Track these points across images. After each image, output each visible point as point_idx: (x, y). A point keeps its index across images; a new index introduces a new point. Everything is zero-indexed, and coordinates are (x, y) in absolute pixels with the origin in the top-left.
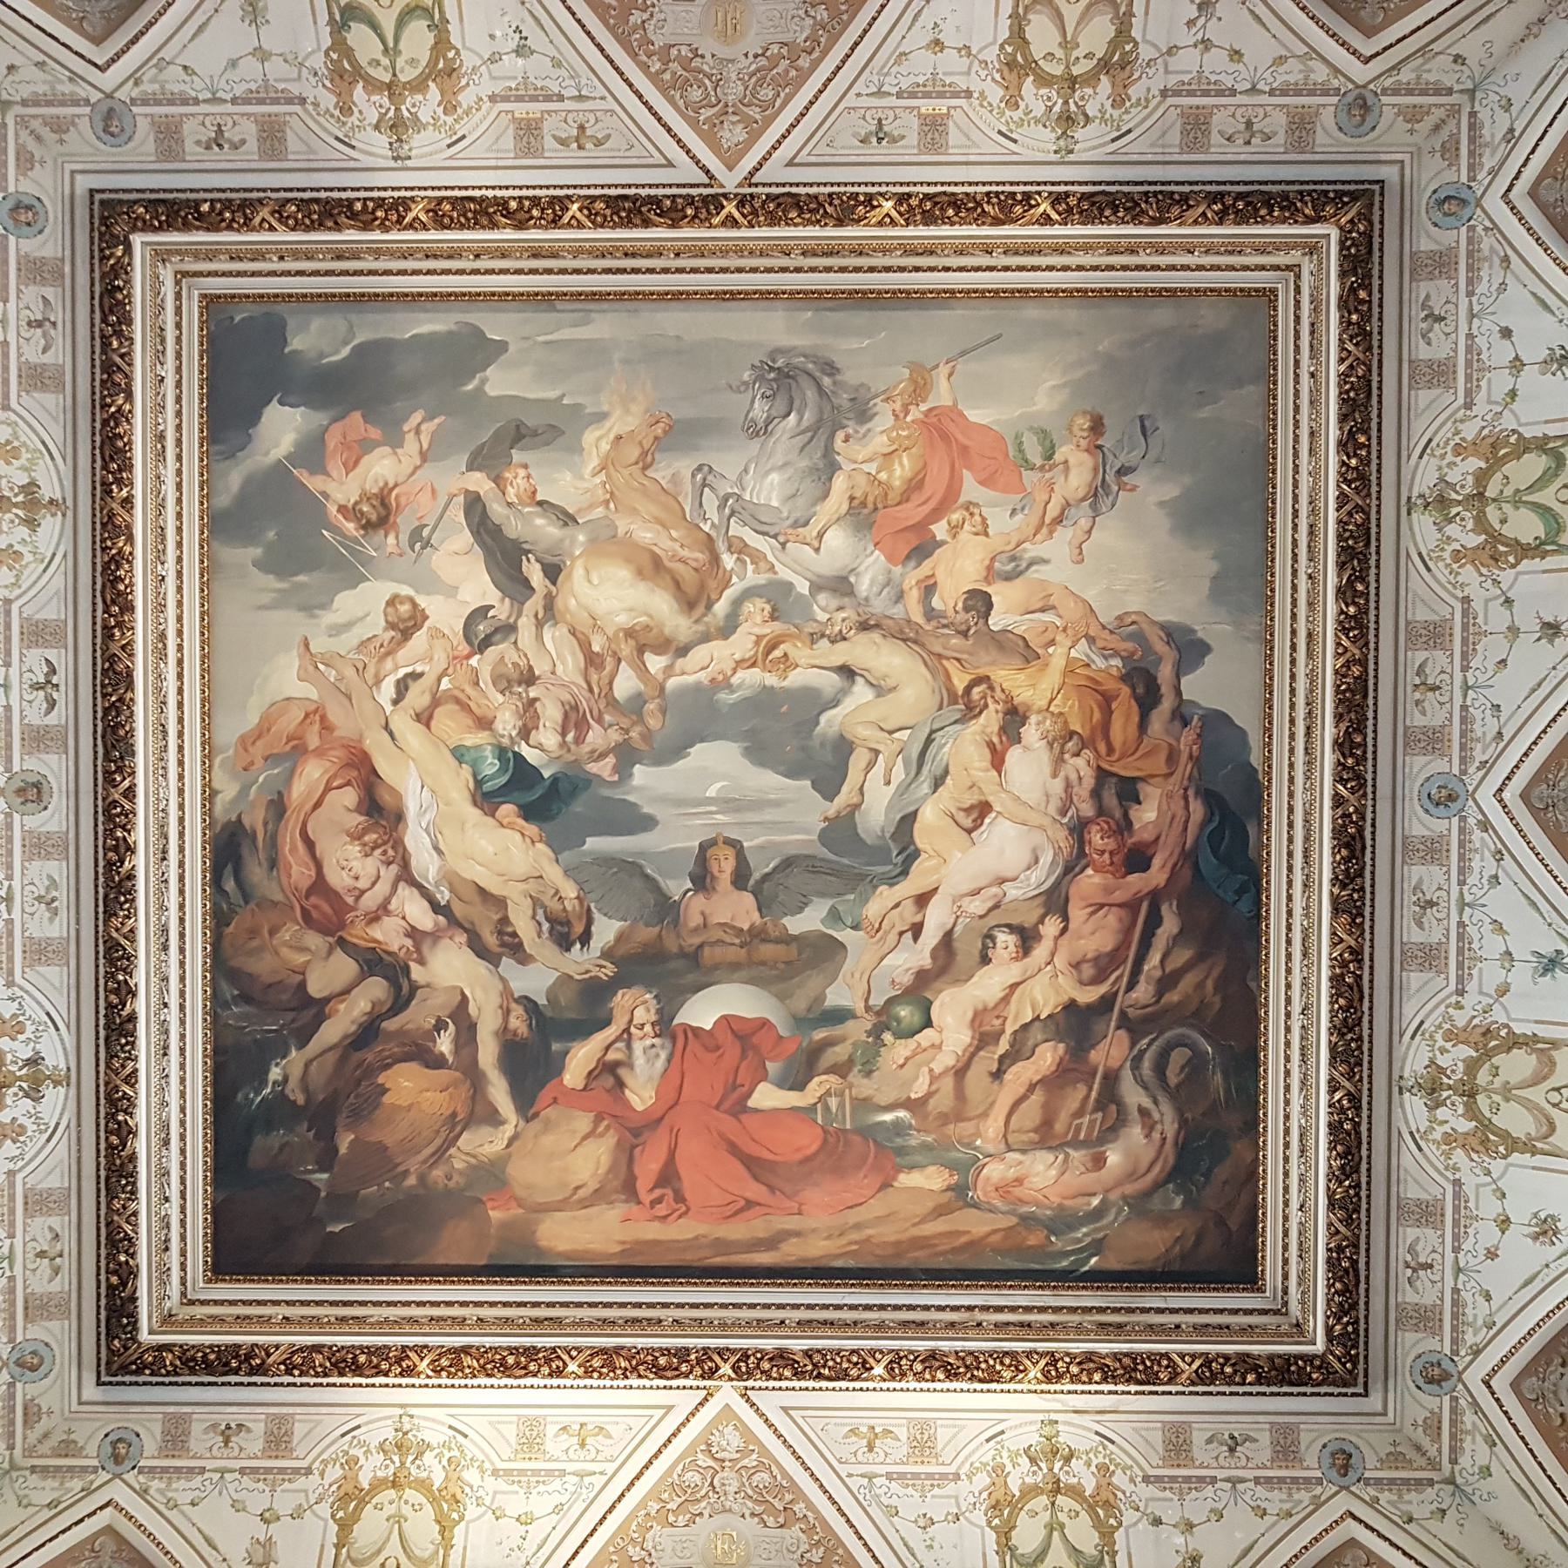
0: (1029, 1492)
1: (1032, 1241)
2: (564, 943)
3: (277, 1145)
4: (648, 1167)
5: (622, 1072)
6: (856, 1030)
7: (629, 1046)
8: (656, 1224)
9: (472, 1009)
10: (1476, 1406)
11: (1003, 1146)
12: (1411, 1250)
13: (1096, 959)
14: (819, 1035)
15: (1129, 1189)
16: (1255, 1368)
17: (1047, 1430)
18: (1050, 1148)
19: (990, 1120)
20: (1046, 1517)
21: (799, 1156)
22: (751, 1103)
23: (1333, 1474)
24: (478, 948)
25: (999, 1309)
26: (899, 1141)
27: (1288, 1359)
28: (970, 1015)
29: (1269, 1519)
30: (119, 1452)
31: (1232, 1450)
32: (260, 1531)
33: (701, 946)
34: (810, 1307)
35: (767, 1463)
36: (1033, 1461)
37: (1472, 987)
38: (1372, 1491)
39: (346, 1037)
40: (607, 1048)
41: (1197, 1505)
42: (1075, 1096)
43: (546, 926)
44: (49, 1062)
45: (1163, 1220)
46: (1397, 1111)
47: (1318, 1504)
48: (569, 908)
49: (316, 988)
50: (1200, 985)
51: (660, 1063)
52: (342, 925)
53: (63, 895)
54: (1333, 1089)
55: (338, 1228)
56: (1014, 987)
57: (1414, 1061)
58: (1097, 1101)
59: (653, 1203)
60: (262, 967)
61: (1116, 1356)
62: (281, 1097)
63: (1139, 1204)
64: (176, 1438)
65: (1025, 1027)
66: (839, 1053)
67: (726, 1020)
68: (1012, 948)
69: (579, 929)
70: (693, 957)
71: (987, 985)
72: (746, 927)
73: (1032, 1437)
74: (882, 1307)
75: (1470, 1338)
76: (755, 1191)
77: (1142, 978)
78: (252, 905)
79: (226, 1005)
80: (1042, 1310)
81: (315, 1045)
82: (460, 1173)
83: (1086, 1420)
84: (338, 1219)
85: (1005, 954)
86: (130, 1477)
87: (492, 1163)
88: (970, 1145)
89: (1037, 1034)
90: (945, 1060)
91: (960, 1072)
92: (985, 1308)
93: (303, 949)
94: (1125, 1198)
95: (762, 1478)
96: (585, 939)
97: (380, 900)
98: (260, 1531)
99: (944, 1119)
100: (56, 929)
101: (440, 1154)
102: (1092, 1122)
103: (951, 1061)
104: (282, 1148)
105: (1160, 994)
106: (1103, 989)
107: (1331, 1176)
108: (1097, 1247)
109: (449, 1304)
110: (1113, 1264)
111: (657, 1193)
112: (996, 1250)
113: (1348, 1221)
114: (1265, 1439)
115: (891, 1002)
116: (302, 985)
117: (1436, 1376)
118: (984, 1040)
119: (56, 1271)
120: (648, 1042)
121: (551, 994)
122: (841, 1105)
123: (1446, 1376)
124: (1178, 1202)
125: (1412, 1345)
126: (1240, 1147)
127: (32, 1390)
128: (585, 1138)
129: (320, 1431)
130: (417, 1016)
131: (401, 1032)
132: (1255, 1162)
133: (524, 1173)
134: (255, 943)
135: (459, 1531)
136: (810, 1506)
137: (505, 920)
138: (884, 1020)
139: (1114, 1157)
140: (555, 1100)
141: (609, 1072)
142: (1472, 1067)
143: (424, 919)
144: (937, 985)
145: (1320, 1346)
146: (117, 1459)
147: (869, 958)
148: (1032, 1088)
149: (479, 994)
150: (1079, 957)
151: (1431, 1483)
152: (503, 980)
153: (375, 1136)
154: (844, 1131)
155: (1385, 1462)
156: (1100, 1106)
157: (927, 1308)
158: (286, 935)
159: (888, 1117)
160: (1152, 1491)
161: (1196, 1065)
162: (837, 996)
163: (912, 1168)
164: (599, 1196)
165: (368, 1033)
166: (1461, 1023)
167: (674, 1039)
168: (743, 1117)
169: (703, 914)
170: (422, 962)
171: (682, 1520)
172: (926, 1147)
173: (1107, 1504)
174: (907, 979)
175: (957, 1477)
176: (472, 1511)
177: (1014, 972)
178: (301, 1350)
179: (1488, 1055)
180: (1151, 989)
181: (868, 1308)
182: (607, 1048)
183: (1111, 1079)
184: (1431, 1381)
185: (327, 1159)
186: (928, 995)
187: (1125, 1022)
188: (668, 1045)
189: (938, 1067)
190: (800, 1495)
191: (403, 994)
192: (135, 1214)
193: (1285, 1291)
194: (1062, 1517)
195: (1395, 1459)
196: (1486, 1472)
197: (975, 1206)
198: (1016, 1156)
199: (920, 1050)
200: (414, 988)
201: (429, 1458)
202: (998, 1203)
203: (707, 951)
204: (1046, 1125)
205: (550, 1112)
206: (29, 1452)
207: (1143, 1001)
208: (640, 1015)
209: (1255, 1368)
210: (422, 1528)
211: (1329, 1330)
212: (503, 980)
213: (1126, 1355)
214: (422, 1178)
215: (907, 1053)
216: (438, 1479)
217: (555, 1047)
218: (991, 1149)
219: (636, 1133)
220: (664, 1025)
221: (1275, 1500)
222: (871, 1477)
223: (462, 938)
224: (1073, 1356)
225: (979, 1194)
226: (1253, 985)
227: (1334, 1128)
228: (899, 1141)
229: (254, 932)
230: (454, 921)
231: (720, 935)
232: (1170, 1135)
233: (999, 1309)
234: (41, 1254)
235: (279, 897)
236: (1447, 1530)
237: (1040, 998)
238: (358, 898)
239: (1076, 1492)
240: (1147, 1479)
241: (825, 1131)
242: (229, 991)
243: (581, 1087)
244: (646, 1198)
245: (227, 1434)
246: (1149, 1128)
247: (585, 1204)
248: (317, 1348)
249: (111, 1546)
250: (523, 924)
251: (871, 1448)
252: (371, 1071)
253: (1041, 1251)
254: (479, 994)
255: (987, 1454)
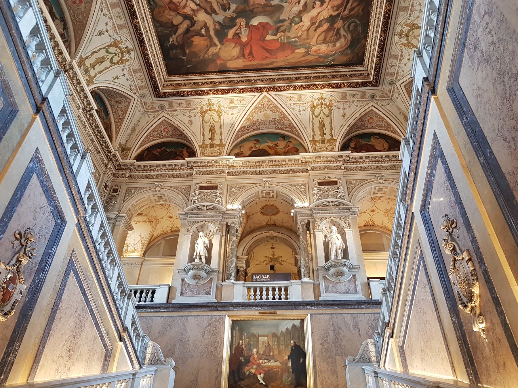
0: (317, 105)
1: (321, 60)
2: (225, 10)
3: (174, 53)
4: (247, 52)
5: (240, 35)
6: (287, 24)
7: (241, 30)
8: (249, 62)
9: (208, 25)
10: (397, 88)
11: (316, 44)
12: (391, 63)
13: (337, 6)
14: (279, 25)
15: (340, 50)
16: (359, 84)
17: (321, 95)
18: (325, 44)
19: (314, 39)
20: (320, 109)
21: (276, 48)
22: (266, 39)
23: (371, 99)
24: (207, 12)
25: (314, 73)
26: (296, 44)
27: (365, 82)
28: (310, 19)
29: (358, 107)
30: (162, 108)
31: (353, 96)
32: (189, 119)
33: (254, 9)
34: (279, 75)
35: (272, 103)
36: (319, 100)
37: (412, 16)
38: (377, 101)
39: (183, 32)
40: (236, 30)
41: (346, 105)
42: (331, 34)
43: (220, 7)
44: (129, 47)
45: (346, 55)
46: (393, 39)
47: (367, 104)
48: (225, 2)
49: (175, 22)
50: (358, 10)
51: (247, 32)
52: (178, 10)
53: (121, 15)
54: (380, 37)
55: (190, 66)
56: (319, 13)
57: (398, 29)
58: (335, 34)
59: (248, 58)
60: (163, 19)
61: (334, 84)
62: (173, 44)
63: (342, 53)
64: (171, 105)
65: (321, 21)
66: (282, 28)
67: (260, 23)
68: (319, 5)
69: (227, 7)
70: (252, 11)
71: (314, 13)
72: (263, 4)
73: (319, 96)
74: (292, 74)
75: (399, 78)
76: (268, 55)
77: (346, 9)
78: (158, 7)
79: (158, 28)
80: (322, 73)
81: (177, 34)
82: (211, 55)
83: (328, 93)
84: (189, 65)
85: (318, 6)
86: (165, 112)
87: (217, 53)
88: (310, 44)
89: (324, 22)
90: (305, 28)
91: (308, 30)
92: (311, 73)
93: (171, 15)
94: (339, 52)
95: (272, 105)
96: (229, 9)
97: (184, 4)
98: (189, 119)
99: (305, 39)
100: (123, 22)
101: (206, 52)
102: (334, 38)
103: (306, 28)
104: (175, 53)
105: (350, 12)
106: (338, 12)
107: (378, 52)
108: (333, 60)
109: (213, 79)
110: (336, 63)
111: (249, 56)
112: (314, 62)
113: (379, 60)
114: (360, 94)
115: (294, 17)
116: (172, 22)
117: (391, 83)
118: (313, 24)
119: (142, 82)
120: (244, 29)
121: (223, 21)
122: (284, 38)
123: (393, 83)
124: (350, 51)
125: (388, 78)
126: (363, 41)
127: (144, 100)
128: (234, 47)
129: (195, 103)
130: (197, 27)
131: (194, 30)
132: (365, 44)
133: (223, 54)
134: (160, 15)
135: (222, 117)
136: (280, 109)
137: (212, 6)
138: (292, 21)
139: (338, 44)
140: (227, 41)
141: (237, 35)
142: (409, 31)
143: (195, 7)
144: (303, 13)
145: (372, 80)
146: (162, 109)
147: (289, 9)
148: (322, 32)
149: (209, 22)
150: (333, 6)
151: (388, 99)
152: (213, 18)
153: (193, 50)
154: (285, 43)
155: (380, 97)
156: (336, 35)
157: (301, 74)
158: (167, 12)
159: (293, 40)
160: (339, 103)
161: (356, 26)
162: (282, 17)
163: (298, 49)
164: (238, 58)
165: (187, 31)
166: (408, 23)
167: (249, 27)
168: (265, 42)
169: (254, 2)
170: (196, 16)
171: (259, 112)
172: (301, 45)
173: (331, 106)
174: (297, 12)
175: (305, 103)
176: (223, 114)
177: (320, 10)
178: (189, 92)
179: (413, 29)
180: (348, 11)
181: (290, 75)
182: (236, 30)
183: (338, 30)
184: (391, 84)
185: (185, 54)
186: (301, 15)
187: (342, 18)
188: (249, 29)
189: (303, 30)
190: (278, 108)
191: (193, 23)
192: (154, 72)
193: (368, 67)
194: (323, 109)
195: (382, 96)
196: (397, 98)
197: (310, 55)
198: (319, 45)
199: (300, 26)
200: (195, 21)
201: (214, 106)
202: (315, 54)
203: (255, 10)
204: (325, 39)
205: (227, 43)
206: (147, 109)
207: (346, 14)
208: (242, 23)
209: (359, 84)
210: (216, 117)
211: (373, 78)
212: (213, 18)
213: (336, 83)
214: (203, 57)
215: (297, 27)
216: (217, 109)
217: (226, 31)
218: (314, 44)
219: (244, 46)
220: (247, 25)
221: (360, 104)
222: (290, 104)
223: (203, 11)
224: (326, 84)
225: (311, 53)
226: (370, 9)
227: (380, 44)
228: (296, 44)
229: (160, 13)
230: (201, 7)
231: (258, 6)
232: (349, 39)
233: (314, 73)
234: (139, 79)
235: (163, 5)
236: (389, 107)
237: (324, 14)
238: (180, 4)
239: (326, 105)
240: (338, 102)
241: (281, 43)
242: (158, 25)
243: (232, 38)
244: (247, 58)
245: (179, 104)
246: (345, 38)
247: (235, 59)
248: (192, 91)
249: (165, 122)
250: (216, 7)
251: (290, 100)
252: (189, 38)
253: (323, 62)
254: (209, 22)
255: (311, 99)
